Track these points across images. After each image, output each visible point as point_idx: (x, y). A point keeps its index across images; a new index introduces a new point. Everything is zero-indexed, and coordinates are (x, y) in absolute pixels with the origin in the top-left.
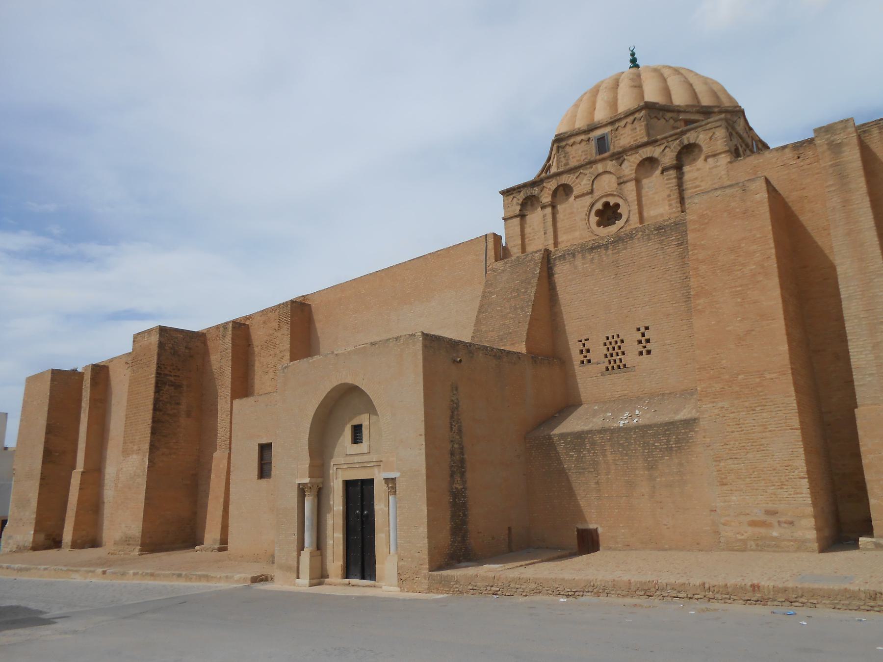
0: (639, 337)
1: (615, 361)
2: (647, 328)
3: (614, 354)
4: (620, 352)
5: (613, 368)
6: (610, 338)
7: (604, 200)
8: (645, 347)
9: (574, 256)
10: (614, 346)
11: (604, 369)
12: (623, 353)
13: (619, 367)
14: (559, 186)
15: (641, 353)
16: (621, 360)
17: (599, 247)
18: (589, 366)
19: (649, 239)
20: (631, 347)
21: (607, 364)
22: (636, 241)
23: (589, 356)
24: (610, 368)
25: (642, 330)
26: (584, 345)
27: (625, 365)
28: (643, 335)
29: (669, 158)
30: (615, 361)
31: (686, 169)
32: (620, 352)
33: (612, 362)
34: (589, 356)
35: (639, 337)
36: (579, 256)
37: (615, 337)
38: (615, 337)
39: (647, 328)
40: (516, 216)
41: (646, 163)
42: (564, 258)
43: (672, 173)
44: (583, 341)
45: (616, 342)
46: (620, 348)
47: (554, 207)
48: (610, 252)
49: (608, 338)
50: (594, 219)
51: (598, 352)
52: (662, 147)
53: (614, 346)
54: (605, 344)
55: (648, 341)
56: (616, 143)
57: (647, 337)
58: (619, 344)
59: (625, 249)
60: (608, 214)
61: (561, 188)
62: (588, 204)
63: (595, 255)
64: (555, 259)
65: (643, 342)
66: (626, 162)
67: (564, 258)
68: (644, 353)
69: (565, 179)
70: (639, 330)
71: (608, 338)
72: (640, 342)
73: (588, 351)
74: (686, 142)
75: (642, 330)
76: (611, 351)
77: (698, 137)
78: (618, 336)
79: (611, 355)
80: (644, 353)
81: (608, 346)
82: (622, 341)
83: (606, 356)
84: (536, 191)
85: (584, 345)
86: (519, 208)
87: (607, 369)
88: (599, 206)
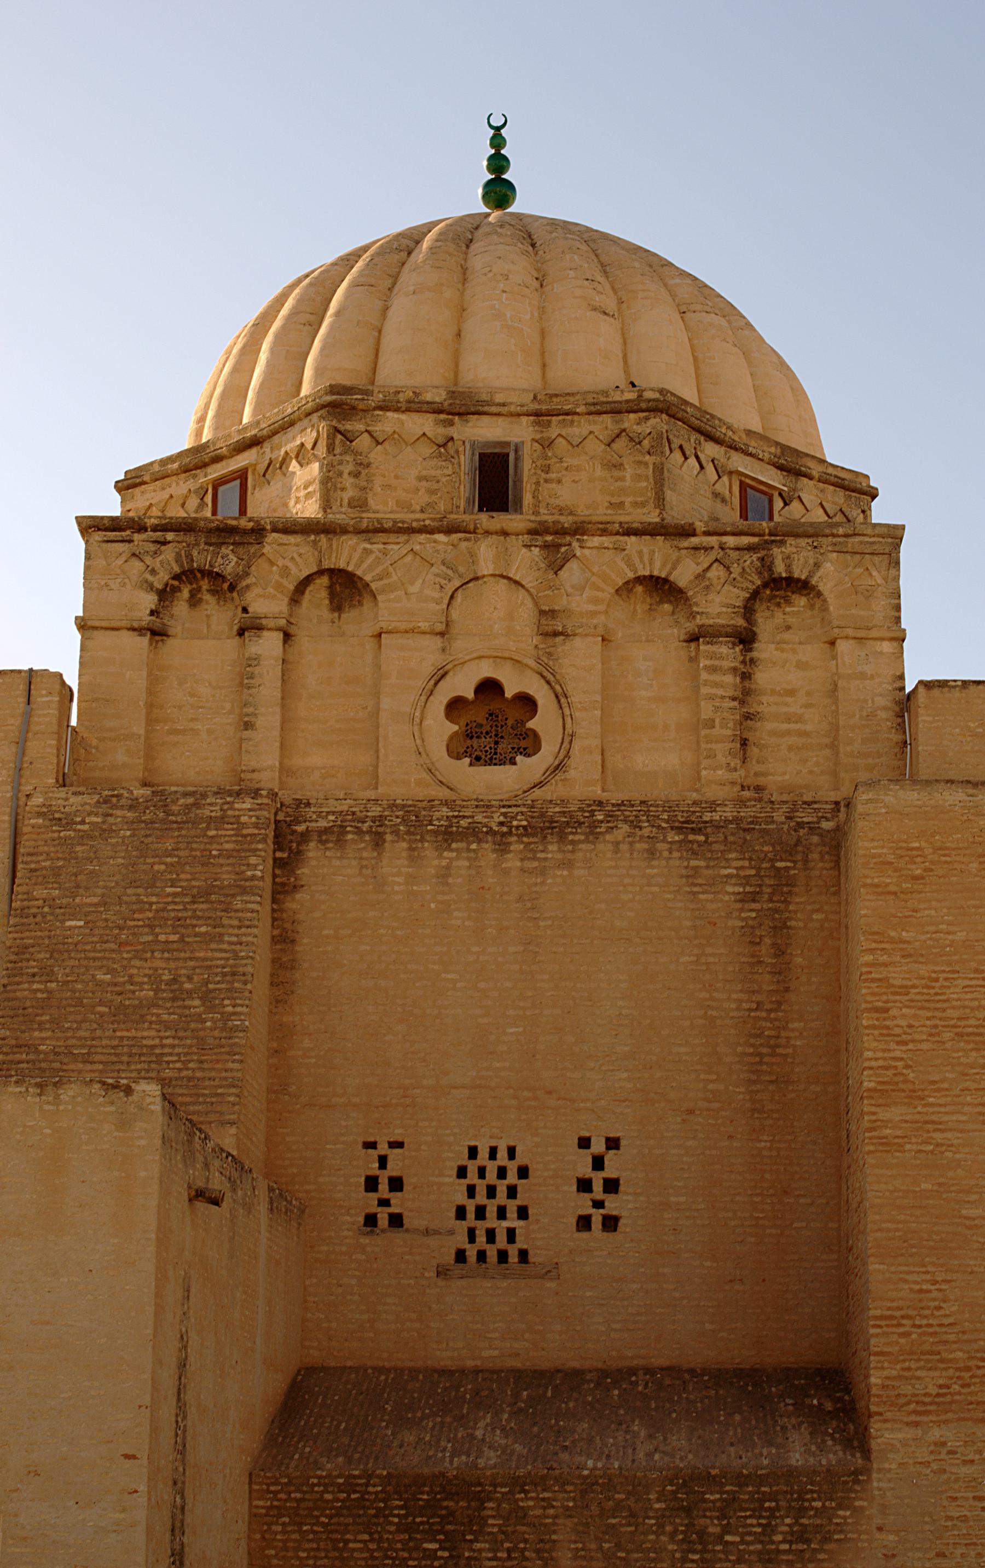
0: (585, 1169)
1: (491, 1235)
2: (613, 1143)
3: (491, 1211)
4: (512, 1207)
5: (482, 1256)
6: (483, 1153)
7: (486, 670)
8: (598, 1204)
9: (378, 841)
10: (493, 1184)
11: (451, 1258)
12: (523, 1213)
13: (503, 1256)
14: (321, 572)
15: (584, 1223)
16: (511, 1233)
17: (473, 833)
18: (398, 1237)
19: (652, 853)
20: (553, 1201)
21: (461, 1240)
22: (604, 847)
23: (398, 1203)
24: (472, 1254)
25: (598, 1146)
26: (383, 1162)
27: (523, 1255)
28: (598, 1163)
29: (719, 604)
30: (491, 1235)
31: (764, 650)
32: (512, 1207)
33: (481, 1238)
34: (398, 1203)
35: (585, 1169)
36: (396, 849)
37: (502, 1154)
38: (502, 1154)
39: (613, 1143)
40: (139, 631)
41: (639, 589)
42: (340, 842)
43: (727, 654)
44: (383, 1149)
45: (502, 1172)
46: (512, 1192)
47: (287, 636)
48: (512, 862)
49: (473, 1152)
50: (441, 728)
51: (433, 1194)
52: (705, 560)
53: (493, 1184)
54: (462, 1172)
55: (612, 1186)
56: (545, 489)
57: (610, 1171)
58: (512, 1178)
59: (569, 865)
60: (493, 721)
61: (324, 580)
62: (428, 668)
63: (457, 860)
64: (305, 837)
65: (598, 1186)
66: (573, 565)
67: (340, 842)
68: (597, 1222)
69: (347, 554)
70: (584, 1143)
71: (473, 1152)
72: (584, 1185)
73: (396, 1184)
74: (780, 569)
75: (598, 1146)
76: (481, 1198)
77: (817, 565)
78: (512, 1152)
79: (481, 1213)
80: (597, 1222)
81: (472, 1177)
82: (523, 1172)
83: (461, 1213)
84: (228, 561)
85: (383, 1162)
86: (149, 600)
87: (461, 1256)
88: (463, 684)
